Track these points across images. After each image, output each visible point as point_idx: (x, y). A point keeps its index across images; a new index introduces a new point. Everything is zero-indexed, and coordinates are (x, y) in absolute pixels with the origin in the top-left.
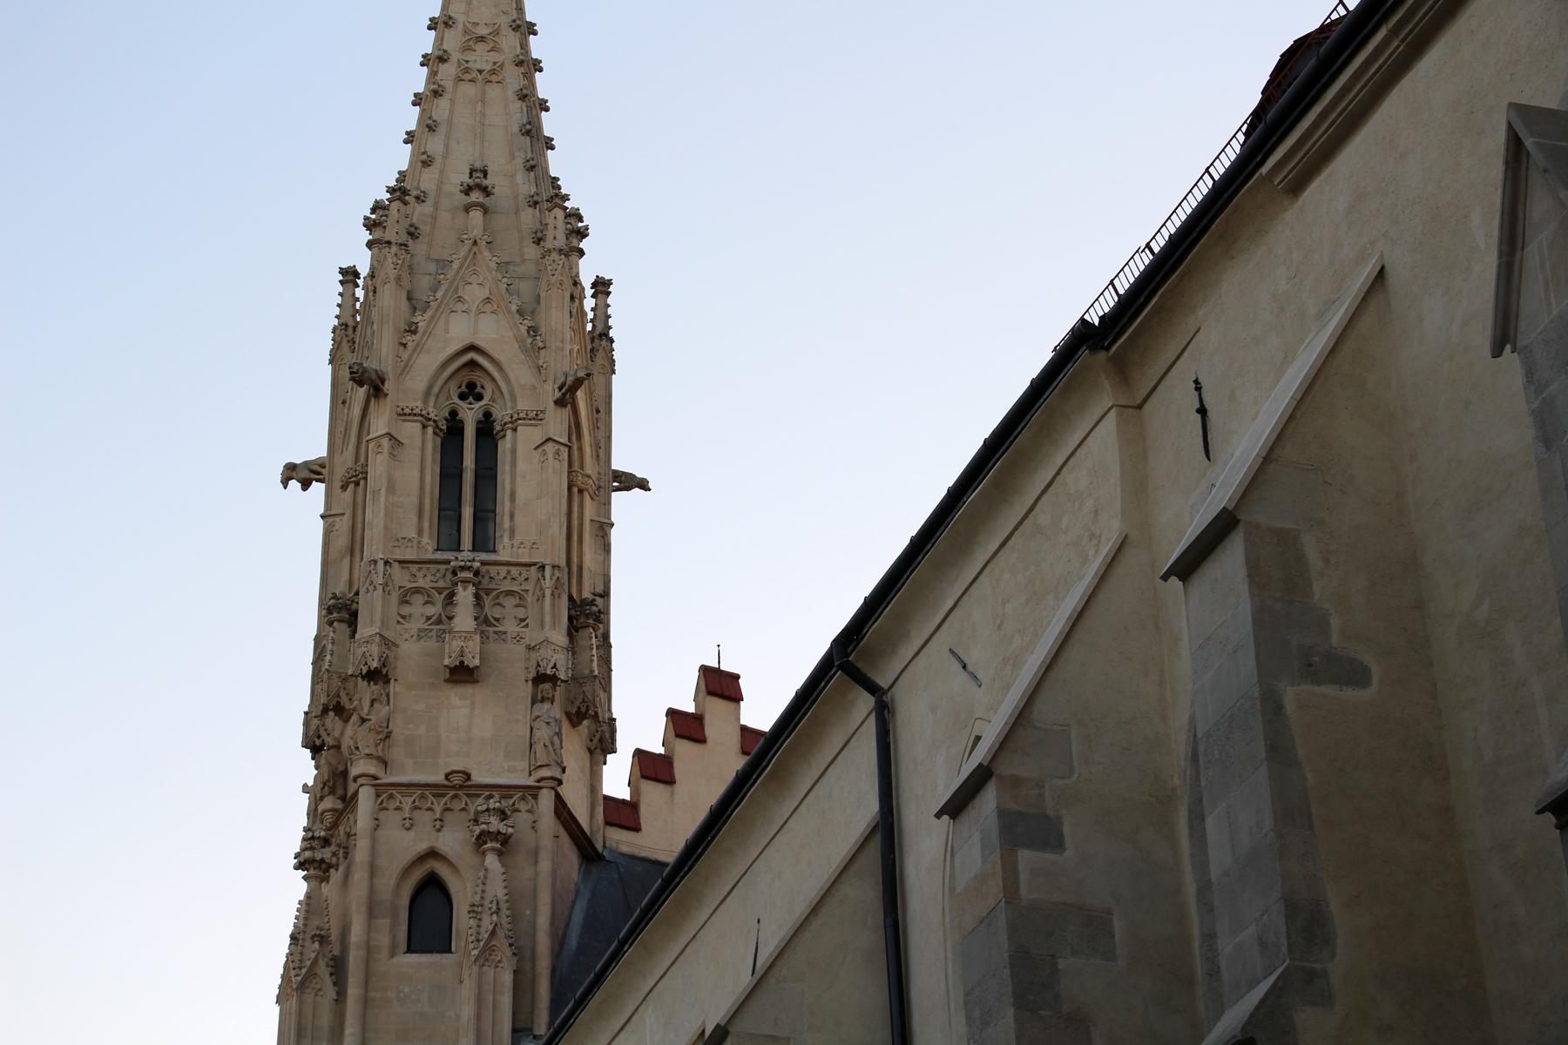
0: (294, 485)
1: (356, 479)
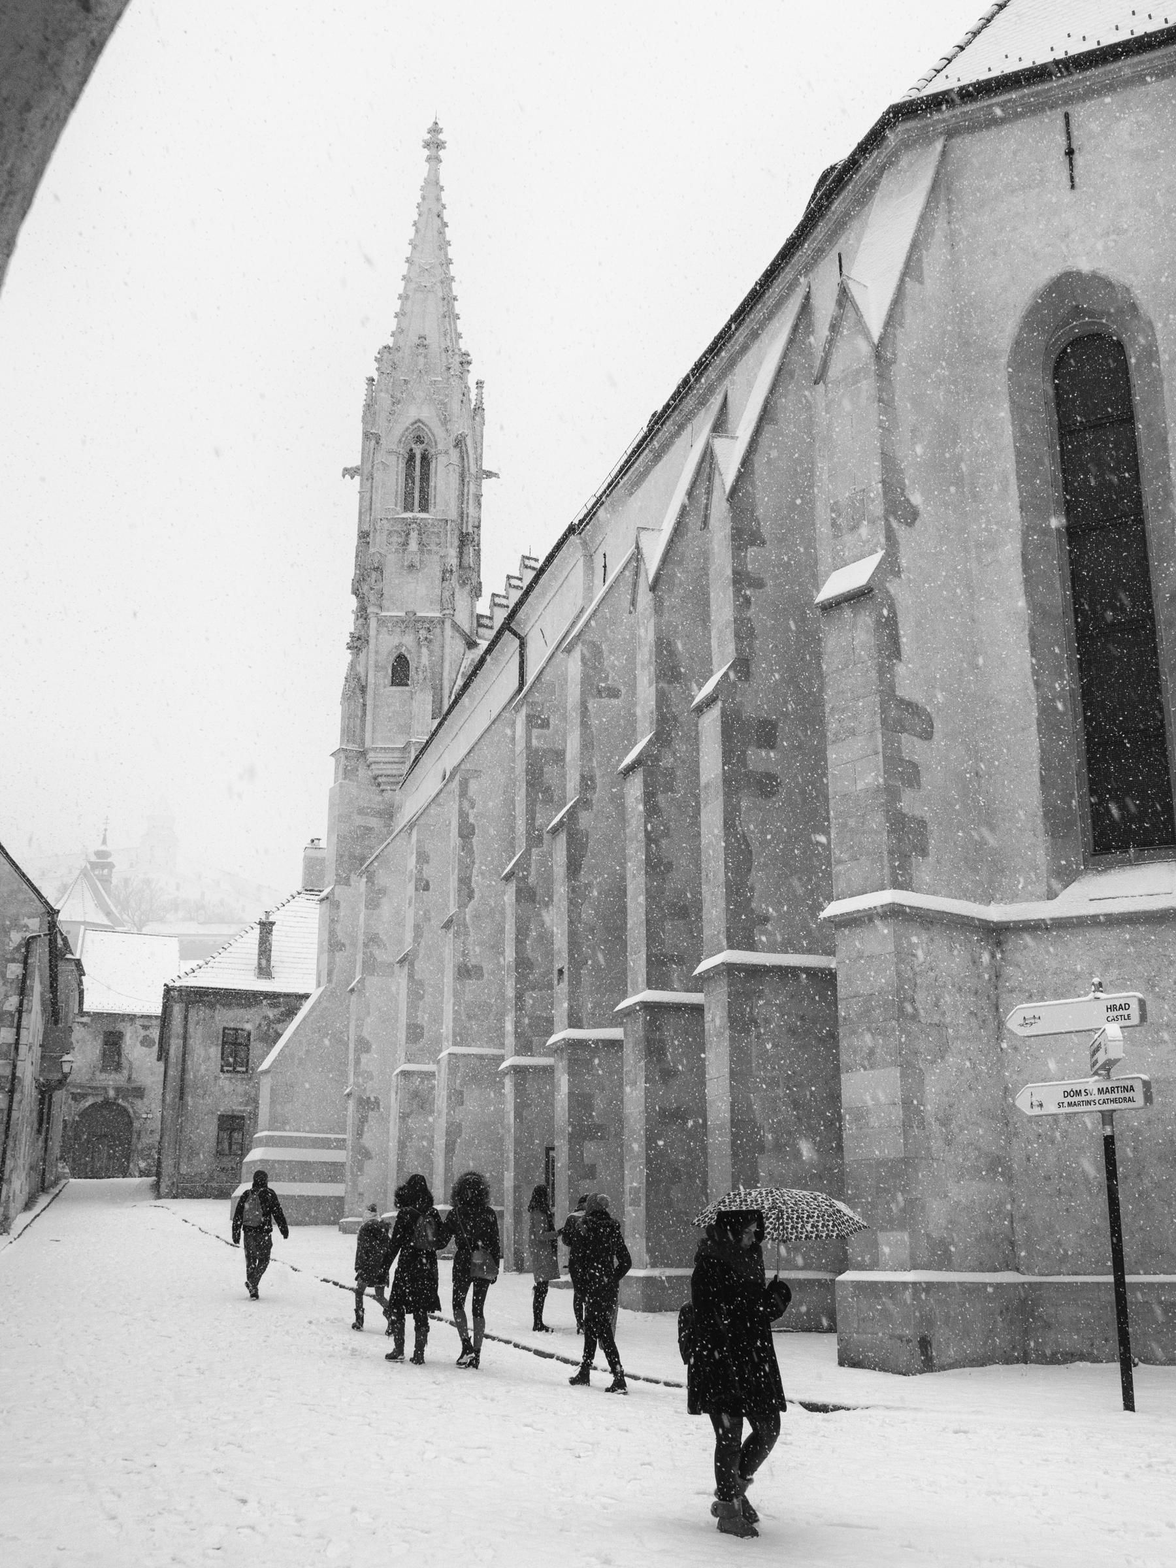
0: (348, 477)
1: (371, 477)
